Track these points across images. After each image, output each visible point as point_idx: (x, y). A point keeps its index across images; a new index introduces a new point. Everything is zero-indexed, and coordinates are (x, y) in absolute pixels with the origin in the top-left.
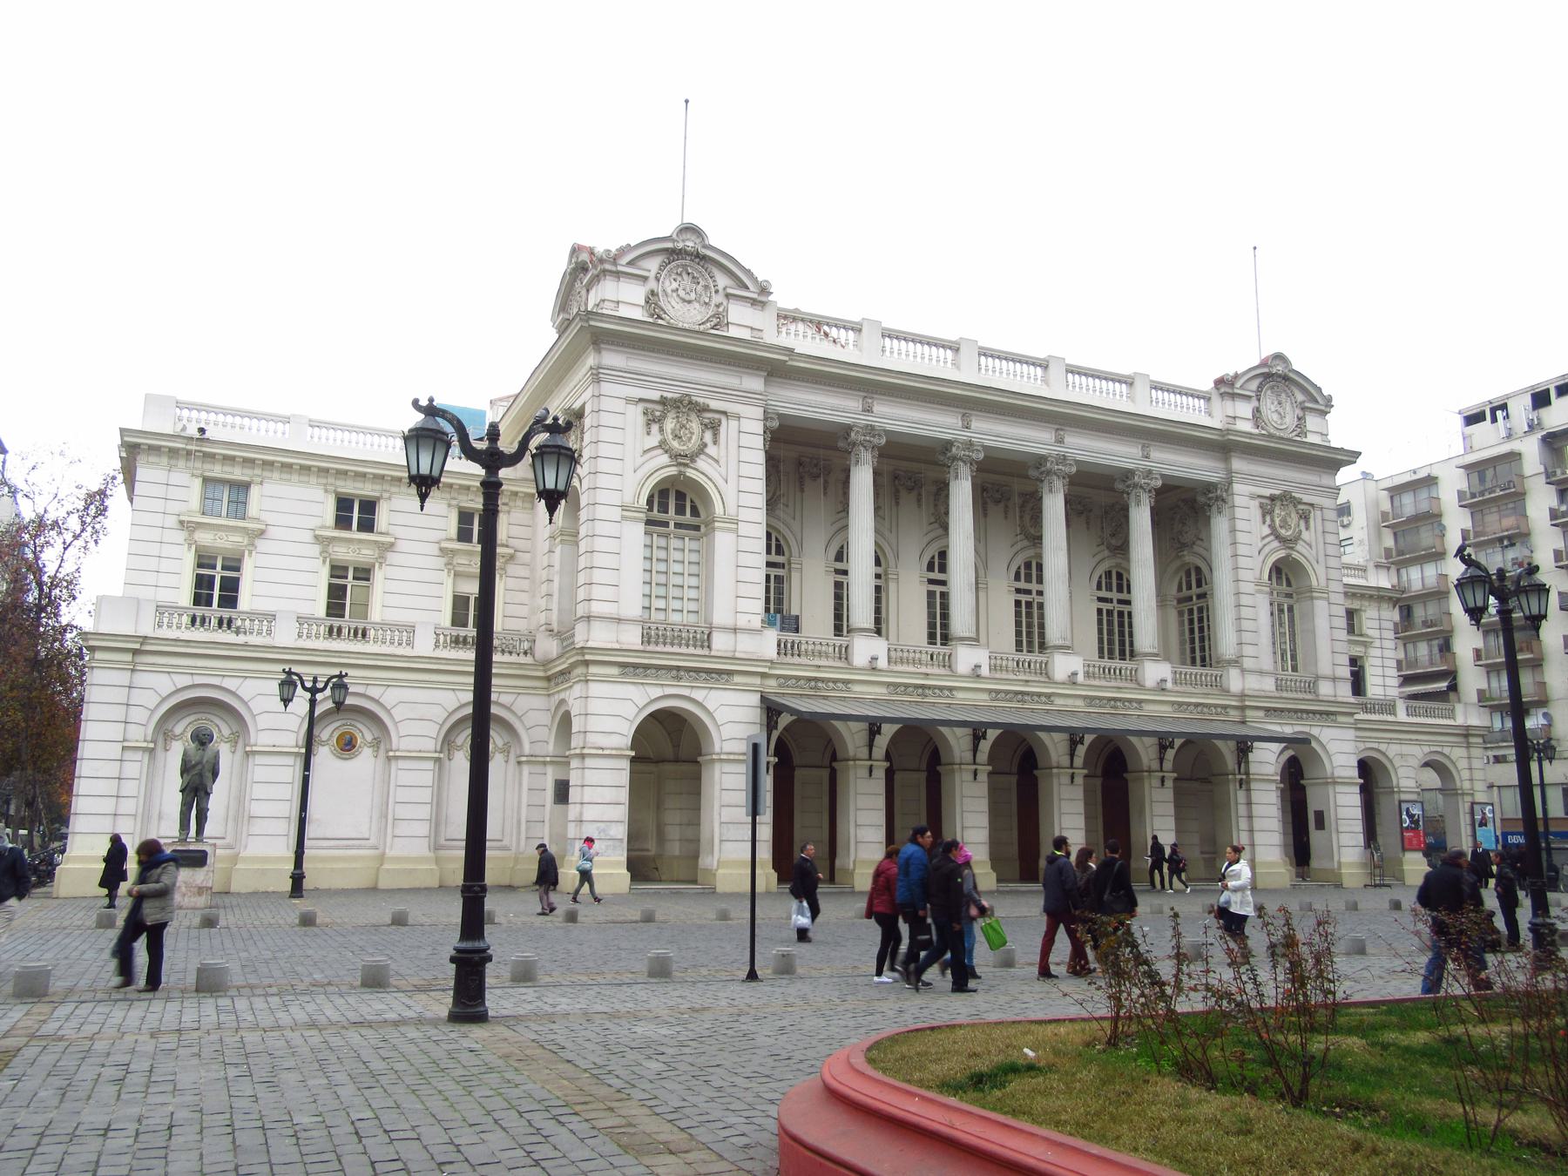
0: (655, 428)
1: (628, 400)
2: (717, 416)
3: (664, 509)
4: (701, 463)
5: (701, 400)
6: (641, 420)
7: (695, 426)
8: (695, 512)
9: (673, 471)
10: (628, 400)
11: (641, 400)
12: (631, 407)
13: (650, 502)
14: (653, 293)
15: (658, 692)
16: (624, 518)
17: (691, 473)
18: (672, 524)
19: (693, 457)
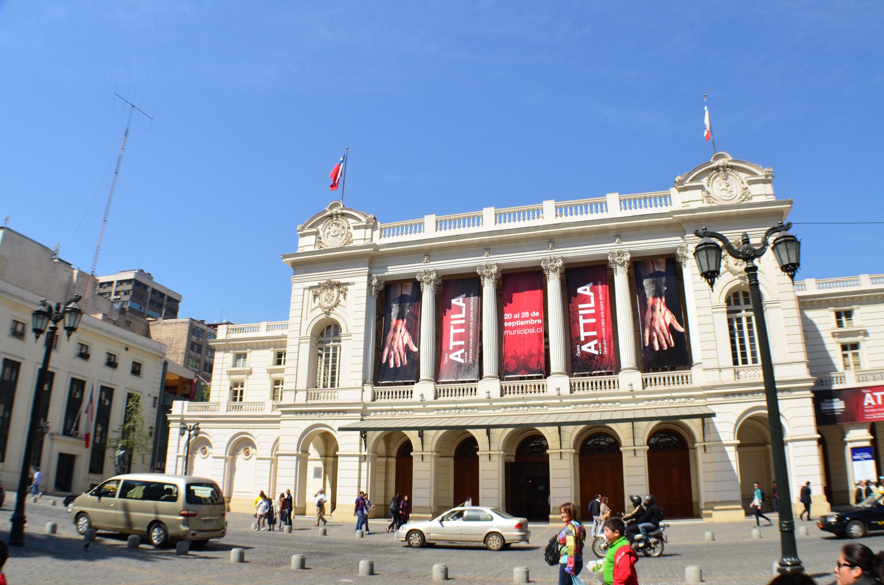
3: (737, 303)
13: (728, 301)
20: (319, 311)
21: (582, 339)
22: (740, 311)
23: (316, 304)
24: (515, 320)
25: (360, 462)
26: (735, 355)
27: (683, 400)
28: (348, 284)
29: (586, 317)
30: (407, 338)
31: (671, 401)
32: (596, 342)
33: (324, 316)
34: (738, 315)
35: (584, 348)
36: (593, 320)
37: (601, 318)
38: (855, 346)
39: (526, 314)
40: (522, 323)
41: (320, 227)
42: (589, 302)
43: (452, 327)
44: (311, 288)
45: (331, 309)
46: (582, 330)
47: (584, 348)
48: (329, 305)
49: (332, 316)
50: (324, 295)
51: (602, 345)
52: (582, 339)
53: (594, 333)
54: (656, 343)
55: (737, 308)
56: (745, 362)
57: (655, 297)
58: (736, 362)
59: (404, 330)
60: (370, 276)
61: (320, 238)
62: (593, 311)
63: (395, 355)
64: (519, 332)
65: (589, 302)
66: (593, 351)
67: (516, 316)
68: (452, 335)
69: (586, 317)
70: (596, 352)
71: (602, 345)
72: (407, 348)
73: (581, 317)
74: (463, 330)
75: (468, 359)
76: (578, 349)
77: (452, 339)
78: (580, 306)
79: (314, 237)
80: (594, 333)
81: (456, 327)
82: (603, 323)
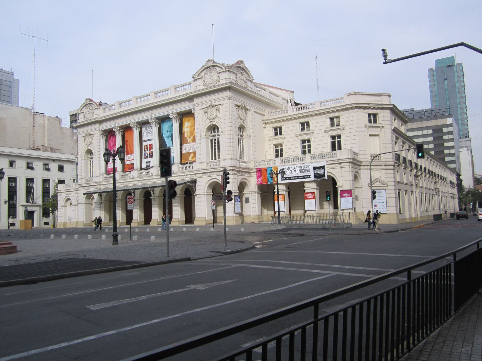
0: (206, 114)
1: (201, 109)
2: (219, 106)
3: (215, 132)
4: (216, 120)
5: (215, 104)
6: (204, 113)
7: (215, 110)
9: (210, 124)
10: (201, 109)
11: (203, 108)
12: (201, 111)
14: (204, 81)
15: (209, 178)
16: (202, 138)
17: (214, 123)
18: (216, 135)
19: (214, 119)
20: (86, 146)
22: (215, 136)
23: (85, 143)
25: (100, 205)
26: (212, 156)
27: (190, 176)
28: (93, 134)
31: (186, 176)
33: (87, 149)
34: (214, 138)
38: (309, 141)
41: (84, 109)
44: (83, 136)
45: (89, 145)
48: (89, 143)
49: (89, 148)
50: (87, 140)
56: (215, 159)
58: (212, 159)
60: (99, 130)
61: (84, 115)
79: (82, 114)
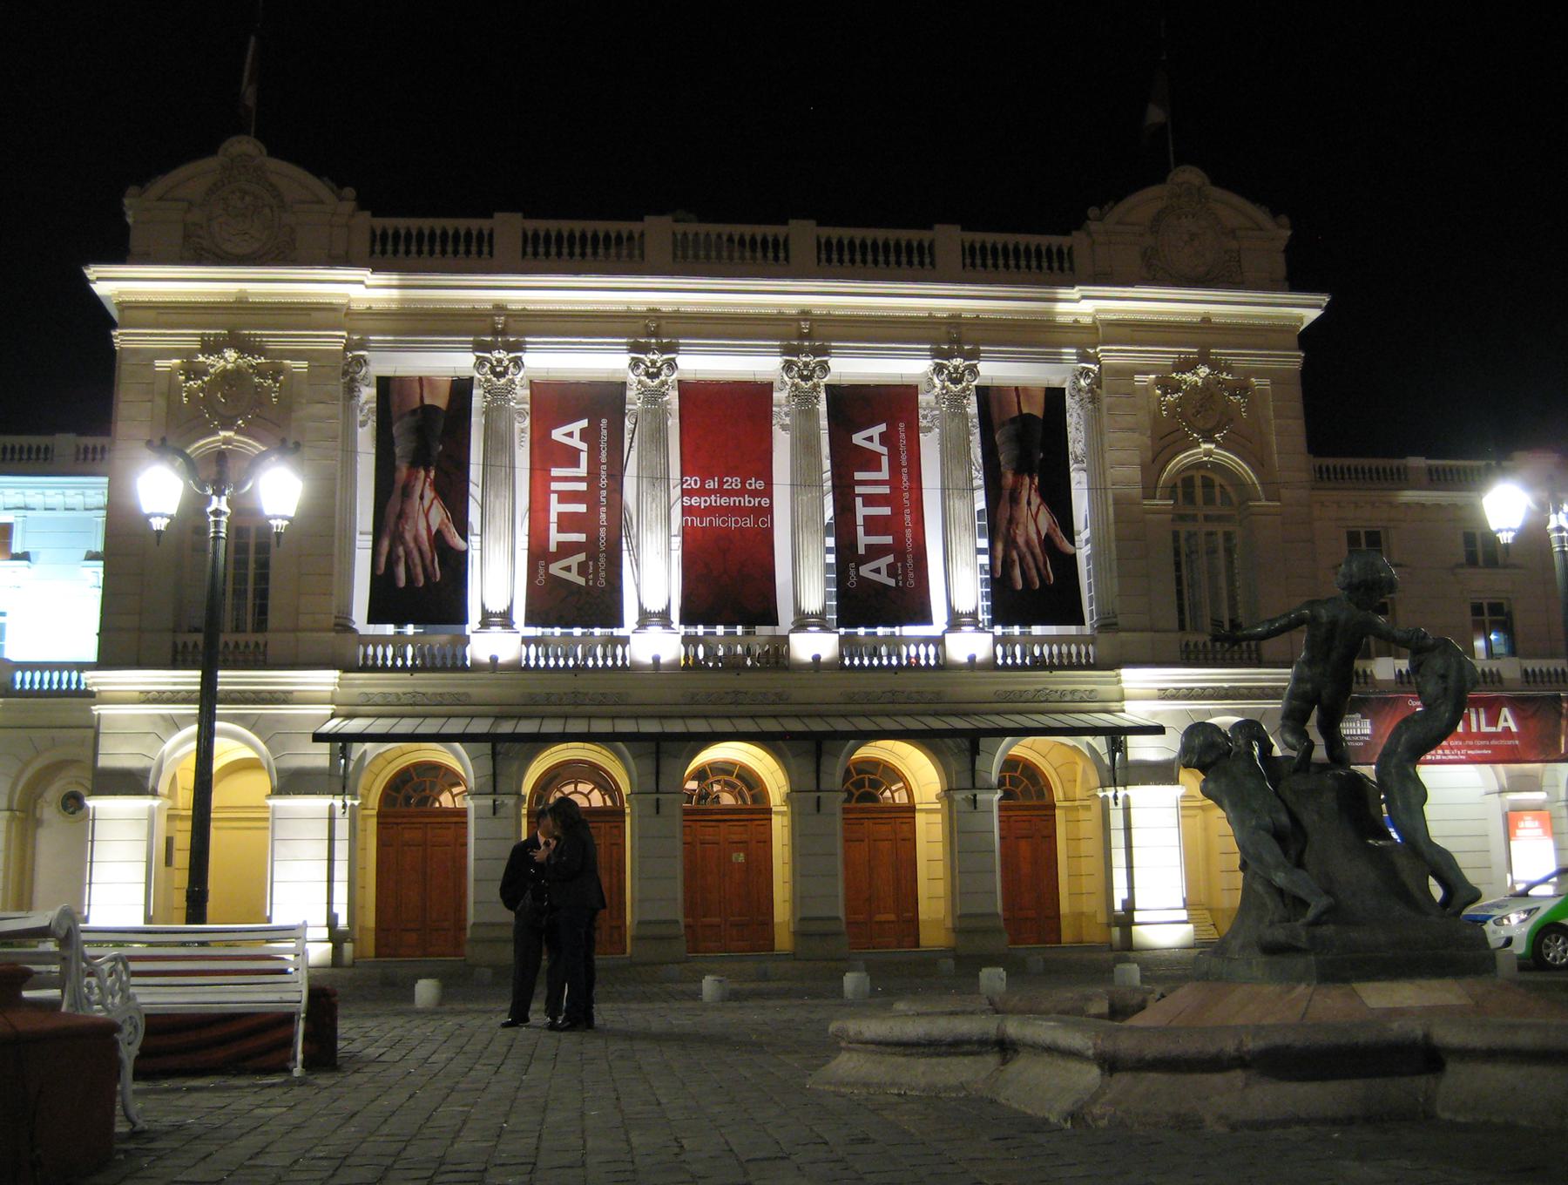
8: (1226, 499)
21: (861, 551)
24: (709, 493)
29: (870, 500)
30: (438, 516)
32: (890, 559)
35: (865, 571)
36: (887, 511)
37: (902, 507)
39: (733, 482)
40: (724, 501)
42: (879, 469)
43: (554, 497)
46: (860, 530)
47: (865, 571)
51: (904, 567)
52: (861, 551)
53: (888, 540)
54: (1017, 572)
55: (1190, 511)
57: (1018, 472)
59: (429, 494)
62: (885, 490)
63: (408, 554)
64: (718, 522)
65: (879, 469)
66: (884, 578)
67: (711, 484)
68: (553, 518)
69: (870, 500)
70: (892, 582)
71: (904, 567)
72: (438, 539)
73: (859, 501)
74: (582, 508)
75: (596, 579)
76: (852, 573)
77: (553, 527)
78: (859, 476)
80: (888, 540)
81: (565, 497)
82: (908, 518)
